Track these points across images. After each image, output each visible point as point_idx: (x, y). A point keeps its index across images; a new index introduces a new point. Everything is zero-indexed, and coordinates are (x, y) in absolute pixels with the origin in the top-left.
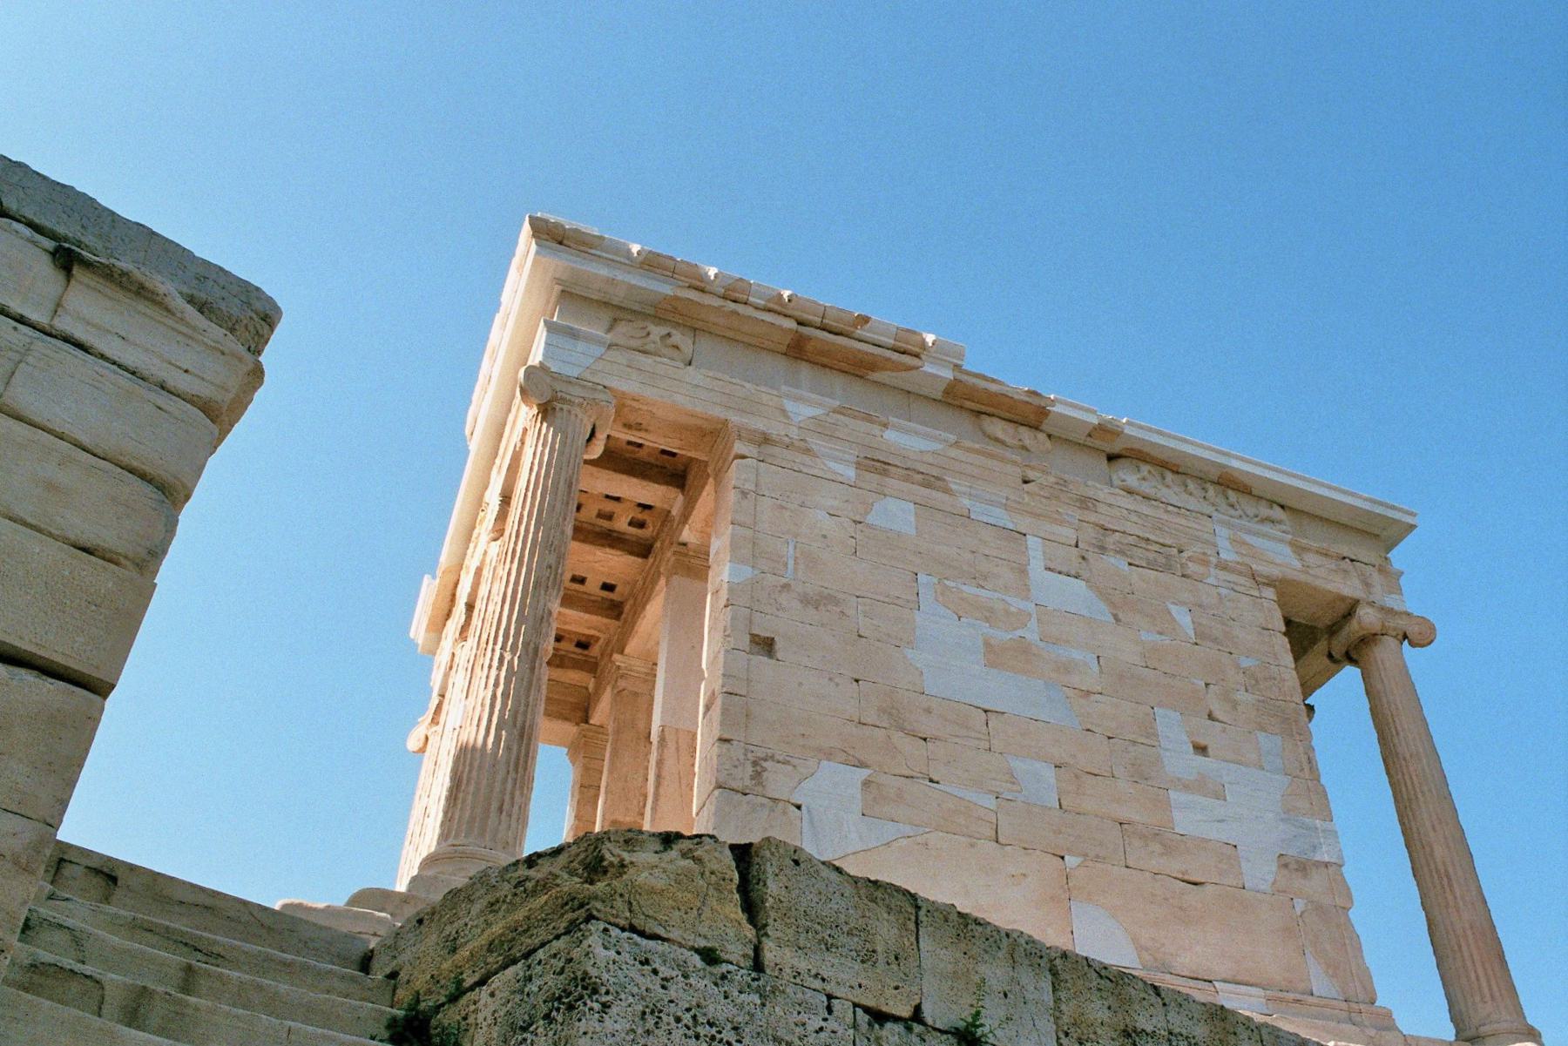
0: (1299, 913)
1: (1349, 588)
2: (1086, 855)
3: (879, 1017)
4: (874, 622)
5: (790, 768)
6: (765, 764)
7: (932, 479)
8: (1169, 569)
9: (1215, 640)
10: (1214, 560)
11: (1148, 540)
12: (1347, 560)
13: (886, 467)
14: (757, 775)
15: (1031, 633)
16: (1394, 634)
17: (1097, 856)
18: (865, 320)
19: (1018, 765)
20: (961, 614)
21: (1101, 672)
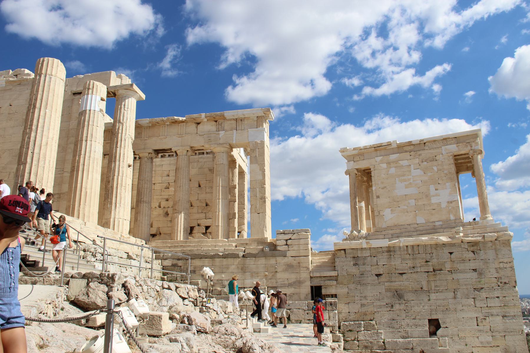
3: (354, 257)
14: (379, 213)
15: (411, 181)
19: (410, 201)
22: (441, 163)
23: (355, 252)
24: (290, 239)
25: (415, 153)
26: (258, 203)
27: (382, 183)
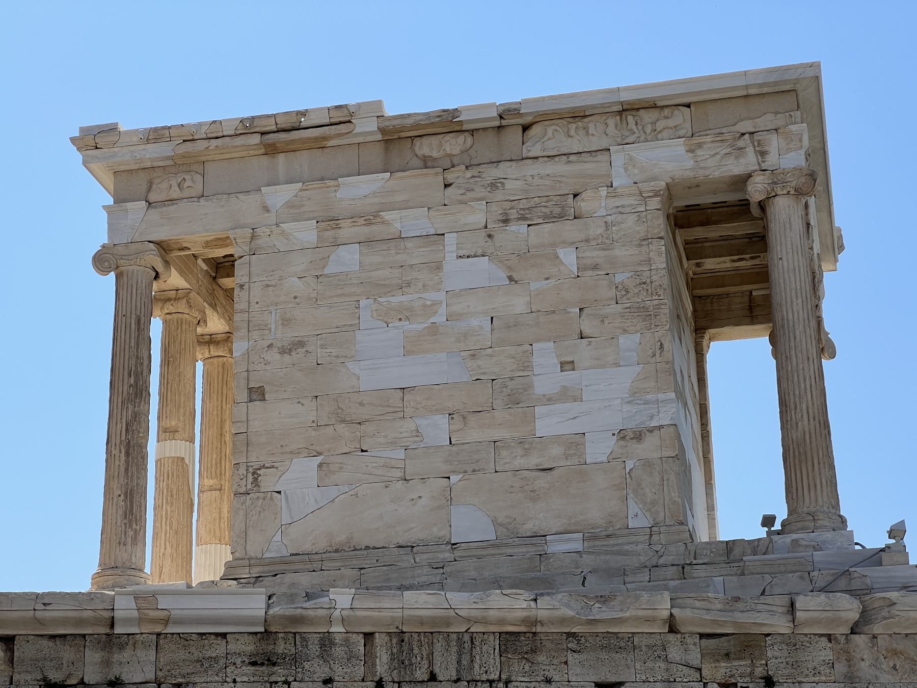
0: (627, 471)
1: (736, 168)
2: (465, 472)
4: (328, 351)
5: (274, 470)
6: (259, 472)
7: (372, 218)
8: (563, 217)
9: (595, 267)
13: (336, 222)
14: (256, 479)
15: (440, 318)
16: (785, 192)
17: (474, 471)
18: (304, 113)
19: (422, 422)
20: (389, 321)
22: (600, 231)
23: (67, 653)
25: (469, 174)
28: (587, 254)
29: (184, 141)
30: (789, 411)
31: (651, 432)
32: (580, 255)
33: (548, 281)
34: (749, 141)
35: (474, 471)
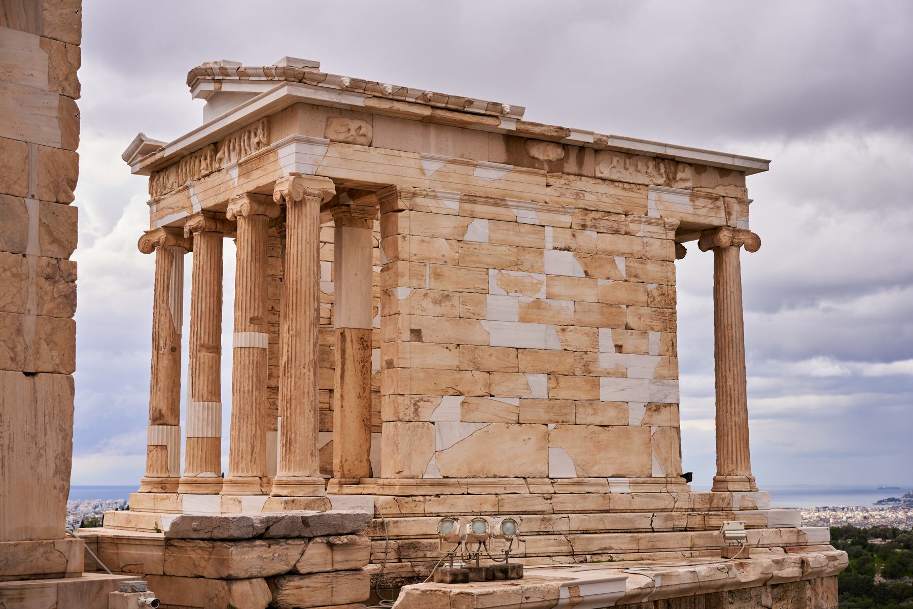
1: (717, 219)
2: (558, 422)
4: (467, 307)
6: (419, 404)
7: (499, 201)
9: (636, 276)
10: (644, 220)
11: (610, 212)
12: (721, 198)
13: (474, 198)
14: (416, 411)
15: (542, 296)
18: (470, 102)
21: (575, 312)
24: (293, 573)
25: (563, 181)
26: (31, 305)
27: (437, 276)
28: (632, 265)
29: (374, 96)
30: (733, 401)
31: (665, 407)
32: (628, 264)
33: (608, 281)
34: (722, 203)
35: (563, 422)
